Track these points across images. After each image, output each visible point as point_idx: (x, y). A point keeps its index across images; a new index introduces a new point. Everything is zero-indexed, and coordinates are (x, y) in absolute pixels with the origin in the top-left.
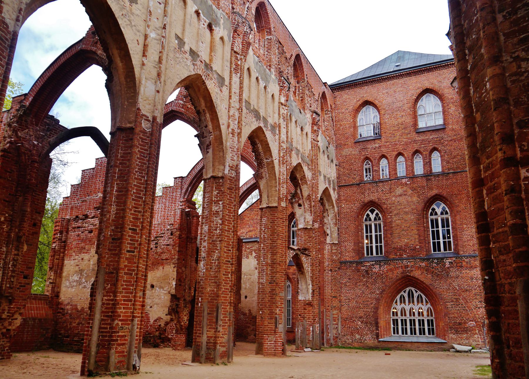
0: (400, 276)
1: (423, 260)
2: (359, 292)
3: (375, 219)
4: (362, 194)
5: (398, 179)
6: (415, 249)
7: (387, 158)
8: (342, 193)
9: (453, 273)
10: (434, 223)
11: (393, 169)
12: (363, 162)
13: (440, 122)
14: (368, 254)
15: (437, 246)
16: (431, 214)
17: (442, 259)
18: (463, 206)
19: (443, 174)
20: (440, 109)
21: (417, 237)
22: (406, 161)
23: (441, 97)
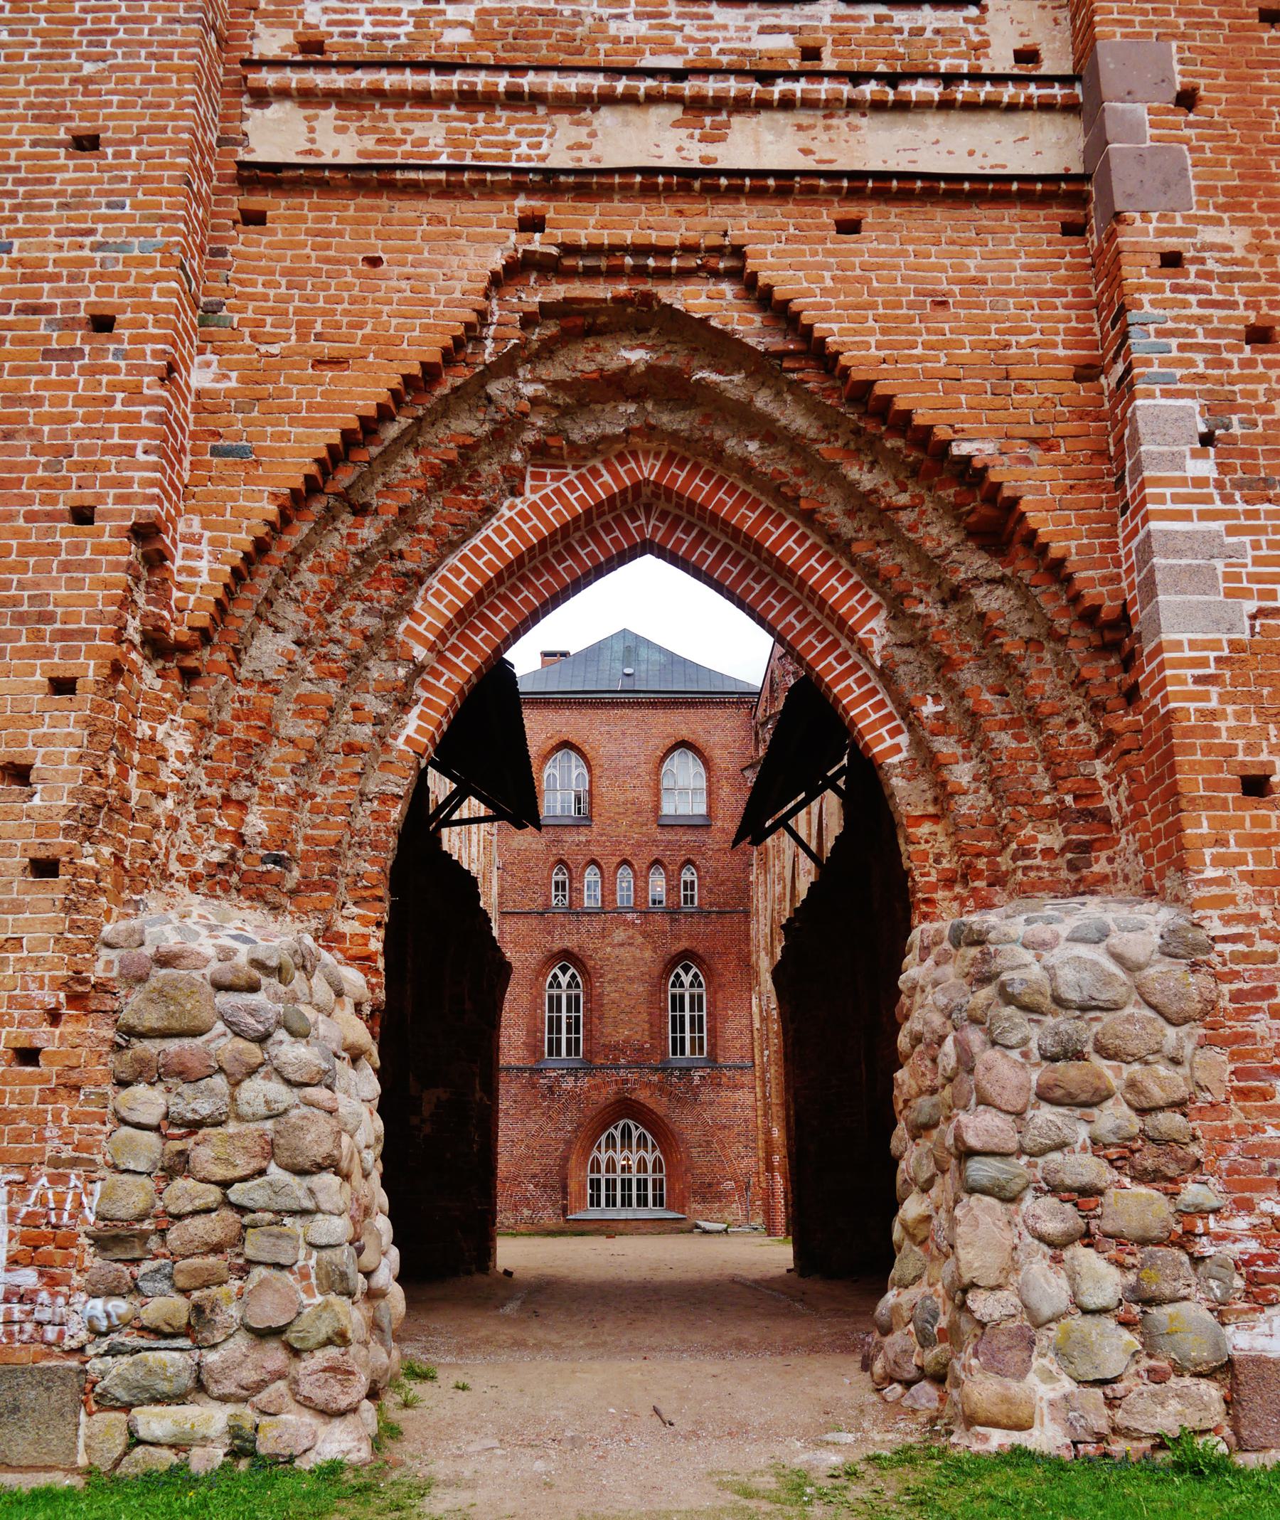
0: (612, 1099)
1: (655, 1070)
2: (533, 1127)
3: (569, 986)
4: (549, 933)
5: (619, 912)
6: (641, 1049)
7: (599, 867)
8: (507, 928)
9: (706, 1095)
10: (678, 1002)
11: (608, 888)
12: (552, 868)
13: (702, 809)
14: (550, 1054)
15: (678, 1046)
16: (674, 985)
17: (689, 1069)
18: (729, 976)
19: (700, 912)
20: (704, 785)
21: (646, 1026)
22: (635, 877)
23: (707, 763)
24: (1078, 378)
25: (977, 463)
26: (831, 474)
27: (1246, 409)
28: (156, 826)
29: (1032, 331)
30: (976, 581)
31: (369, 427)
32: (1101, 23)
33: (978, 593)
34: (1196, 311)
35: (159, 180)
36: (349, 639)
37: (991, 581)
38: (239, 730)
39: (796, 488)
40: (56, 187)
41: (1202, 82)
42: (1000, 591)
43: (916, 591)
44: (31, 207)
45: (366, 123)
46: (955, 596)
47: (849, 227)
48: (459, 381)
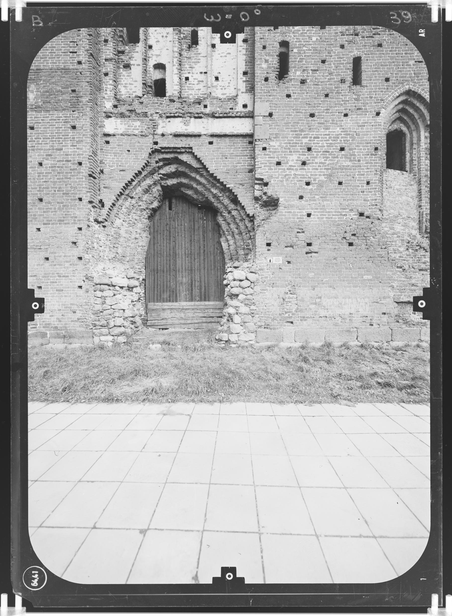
24: (249, 172)
25: (230, 189)
26: (209, 190)
27: (274, 178)
28: (100, 251)
29: (241, 163)
30: (232, 209)
31: (130, 182)
32: (257, 98)
33: (233, 212)
34: (268, 159)
35: (87, 135)
36: (133, 220)
37: (235, 209)
38: (115, 236)
39: (205, 193)
40: (69, 137)
41: (273, 111)
42: (236, 211)
43: (224, 211)
44: (65, 141)
45: (126, 122)
46: (229, 212)
47: (211, 143)
48: (145, 174)
